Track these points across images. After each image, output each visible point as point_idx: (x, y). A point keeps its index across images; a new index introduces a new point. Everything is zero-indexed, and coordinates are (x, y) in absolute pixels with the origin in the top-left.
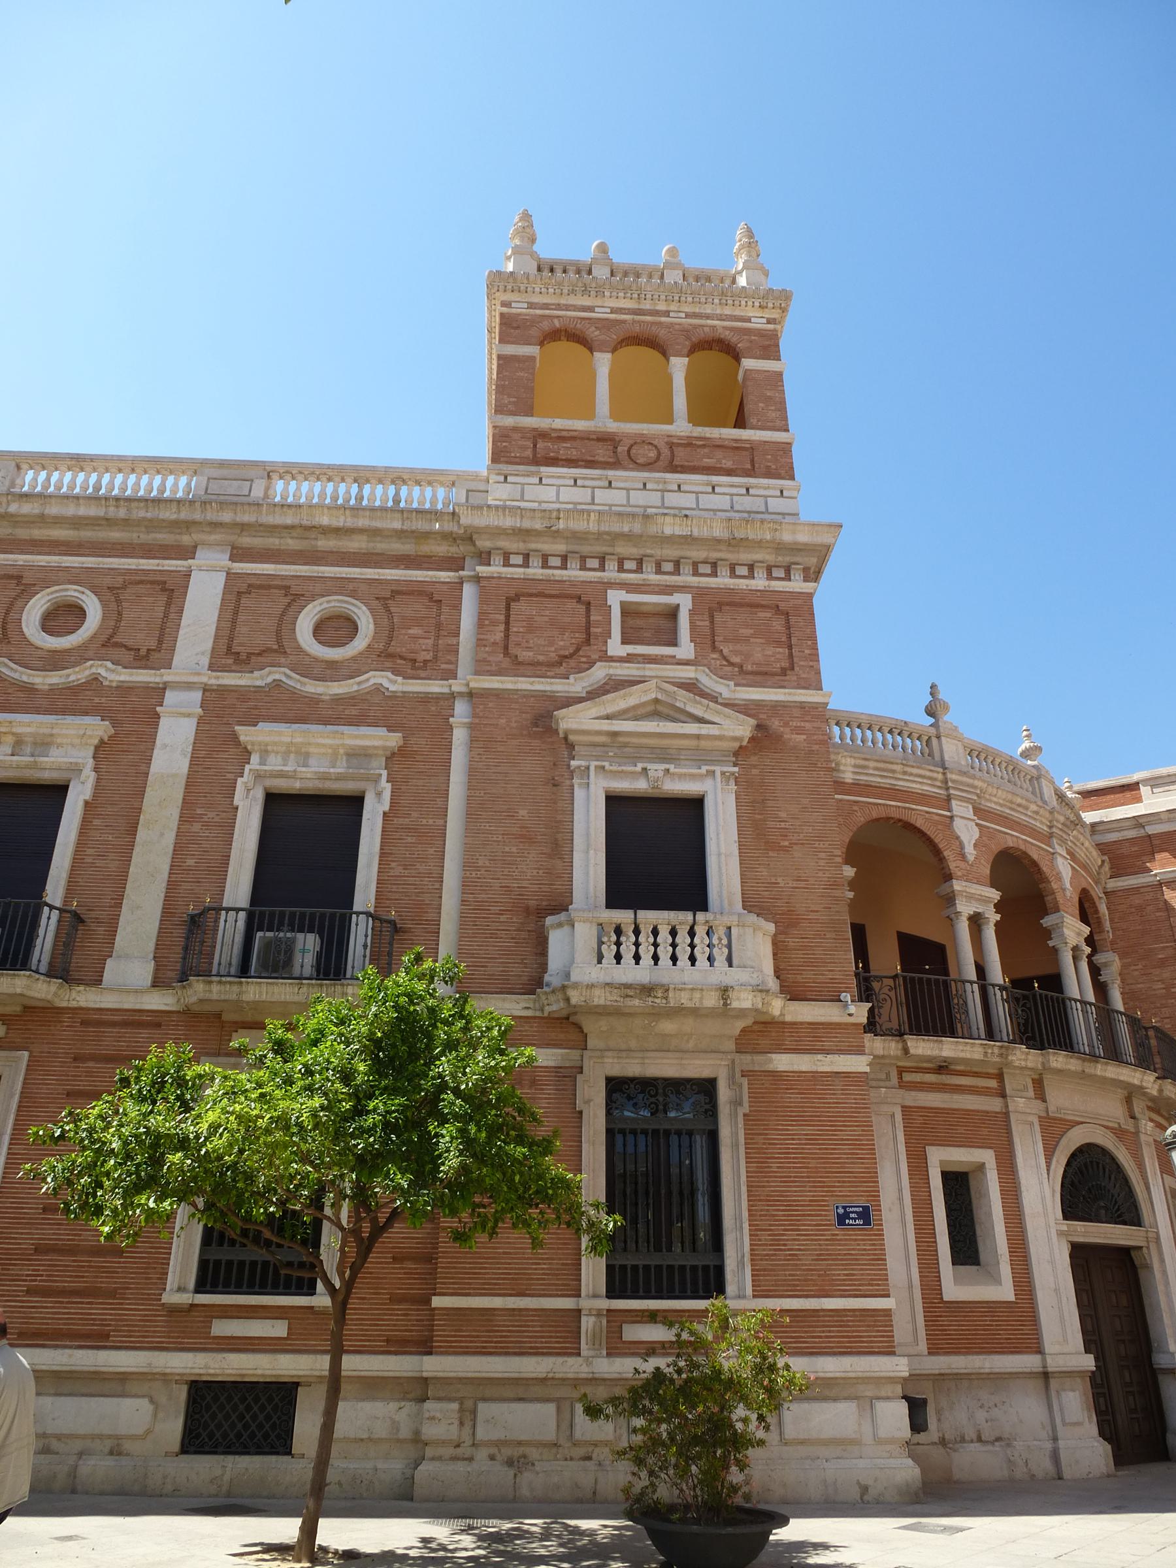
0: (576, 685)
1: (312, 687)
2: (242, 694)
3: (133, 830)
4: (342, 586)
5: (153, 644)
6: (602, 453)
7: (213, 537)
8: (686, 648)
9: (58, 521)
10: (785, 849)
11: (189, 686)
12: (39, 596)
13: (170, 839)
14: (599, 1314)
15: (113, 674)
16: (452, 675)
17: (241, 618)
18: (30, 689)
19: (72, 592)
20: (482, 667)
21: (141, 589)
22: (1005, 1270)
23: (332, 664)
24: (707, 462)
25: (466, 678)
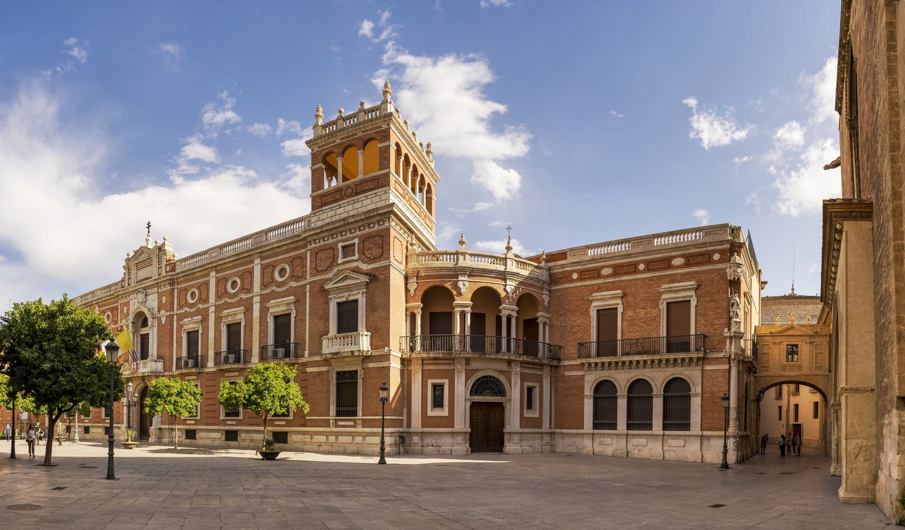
1: (279, 290)
16: (306, 278)
20: (312, 275)
25: (309, 279)
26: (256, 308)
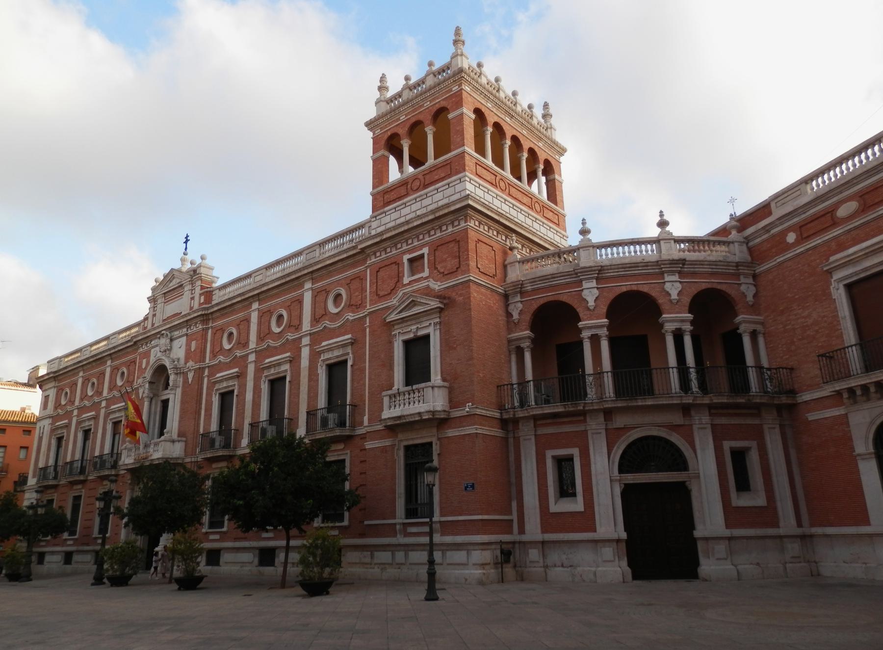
0: (394, 301)
4: (338, 283)
6: (403, 191)
8: (426, 273)
10: (455, 348)
14: (400, 524)
20: (372, 303)
22: (580, 497)
24: (436, 177)
25: (369, 308)
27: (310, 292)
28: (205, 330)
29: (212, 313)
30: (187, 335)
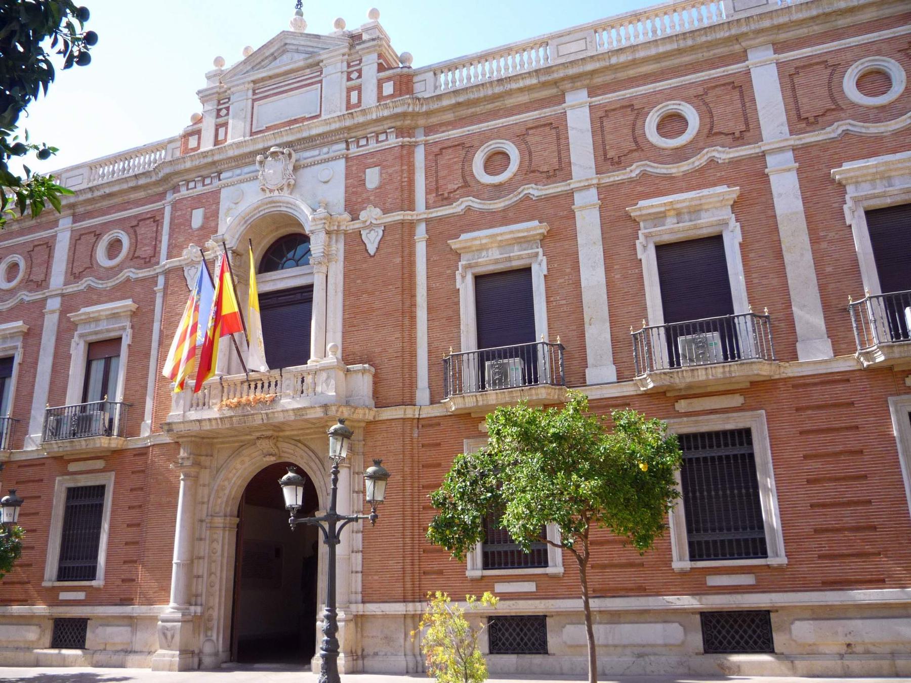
1: (874, 129)
2: (822, 146)
3: (779, 255)
5: (743, 128)
7: (757, 41)
9: (646, 60)
11: (781, 150)
12: (651, 114)
13: (809, 256)
15: (723, 154)
17: (799, 93)
18: (670, 178)
19: (672, 106)
21: (718, 91)
23: (882, 108)
26: (786, 192)
27: (773, 70)
28: (409, 149)
29: (428, 114)
30: (347, 158)
